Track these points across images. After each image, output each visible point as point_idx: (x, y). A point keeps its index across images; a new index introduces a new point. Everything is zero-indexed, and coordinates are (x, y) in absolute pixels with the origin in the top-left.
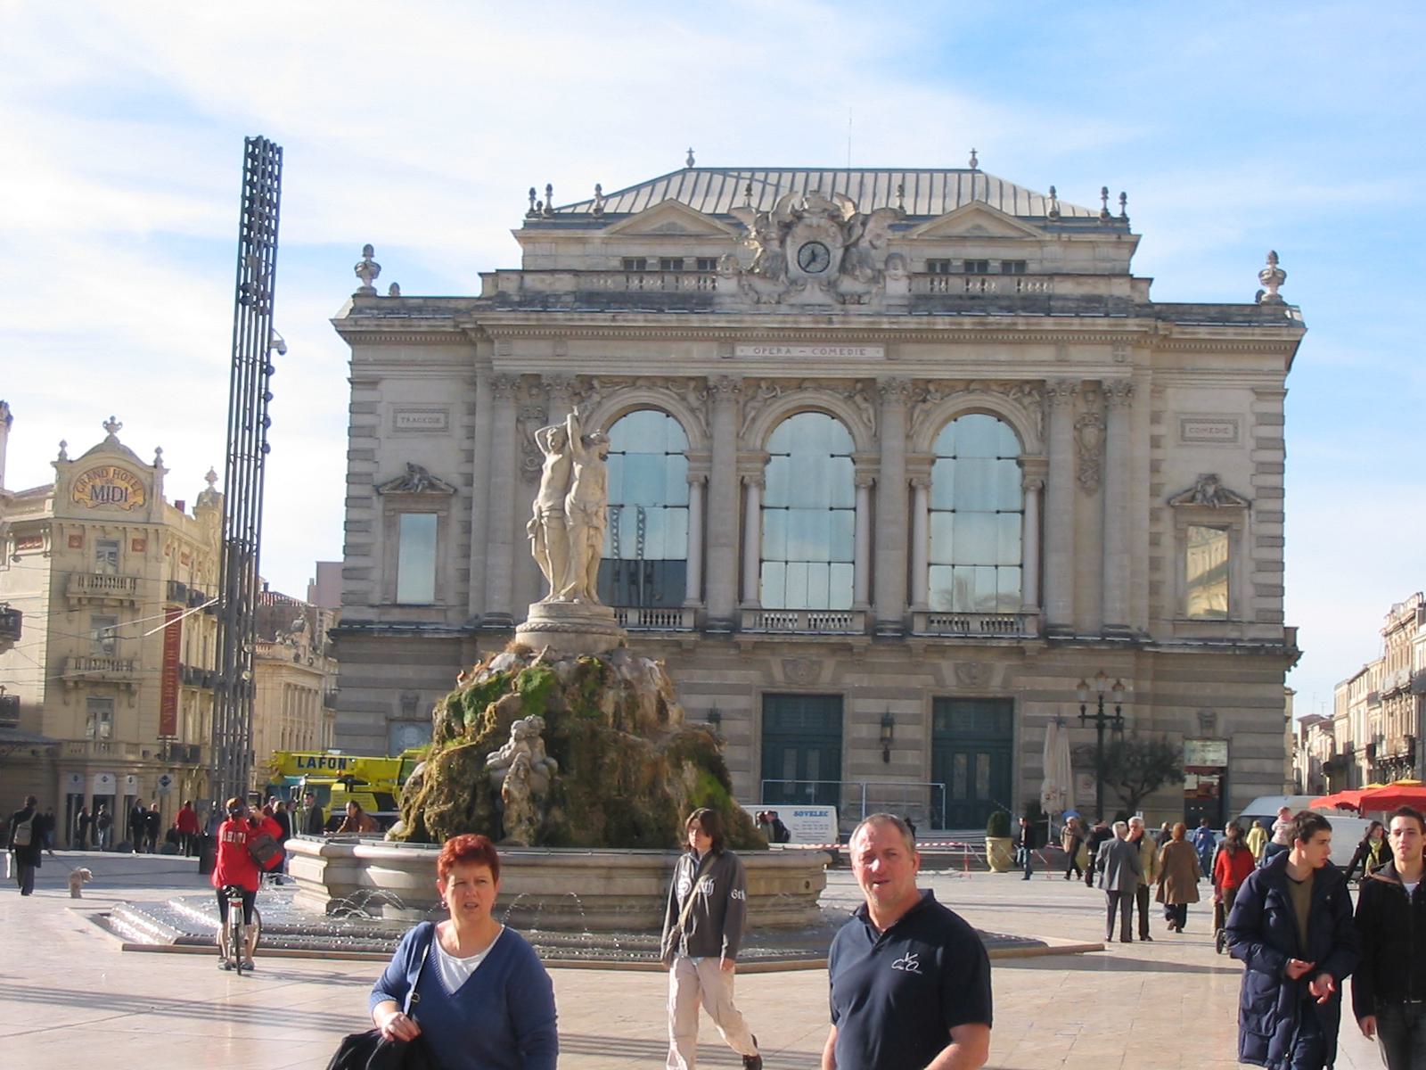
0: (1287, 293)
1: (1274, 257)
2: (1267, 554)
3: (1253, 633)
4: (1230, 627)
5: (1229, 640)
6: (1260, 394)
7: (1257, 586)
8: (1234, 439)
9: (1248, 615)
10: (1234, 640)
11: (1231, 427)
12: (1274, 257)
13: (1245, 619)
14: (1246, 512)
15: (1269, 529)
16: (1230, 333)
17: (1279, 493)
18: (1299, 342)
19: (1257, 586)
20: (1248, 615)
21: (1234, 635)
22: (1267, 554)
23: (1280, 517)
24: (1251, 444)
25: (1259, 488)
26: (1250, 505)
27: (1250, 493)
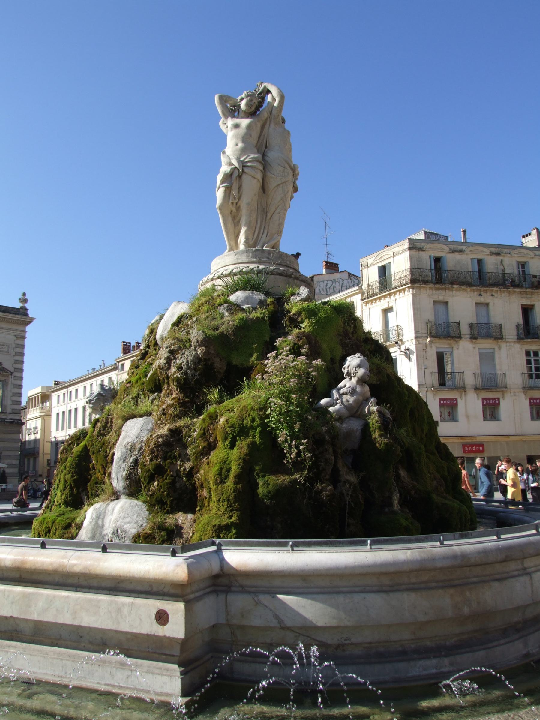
0: (27, 306)
1: (24, 294)
2: (16, 390)
3: (10, 416)
4: (3, 414)
5: (2, 419)
6: (18, 337)
7: (13, 401)
8: (8, 352)
9: (9, 410)
10: (5, 419)
11: (7, 348)
12: (24, 294)
13: (8, 412)
14: (10, 376)
15: (18, 382)
16: (10, 316)
17: (21, 370)
18: (31, 322)
19: (13, 401)
20: (9, 410)
21: (4, 417)
22: (16, 390)
23: (21, 378)
24: (13, 353)
25: (15, 369)
26: (12, 373)
27: (12, 370)
